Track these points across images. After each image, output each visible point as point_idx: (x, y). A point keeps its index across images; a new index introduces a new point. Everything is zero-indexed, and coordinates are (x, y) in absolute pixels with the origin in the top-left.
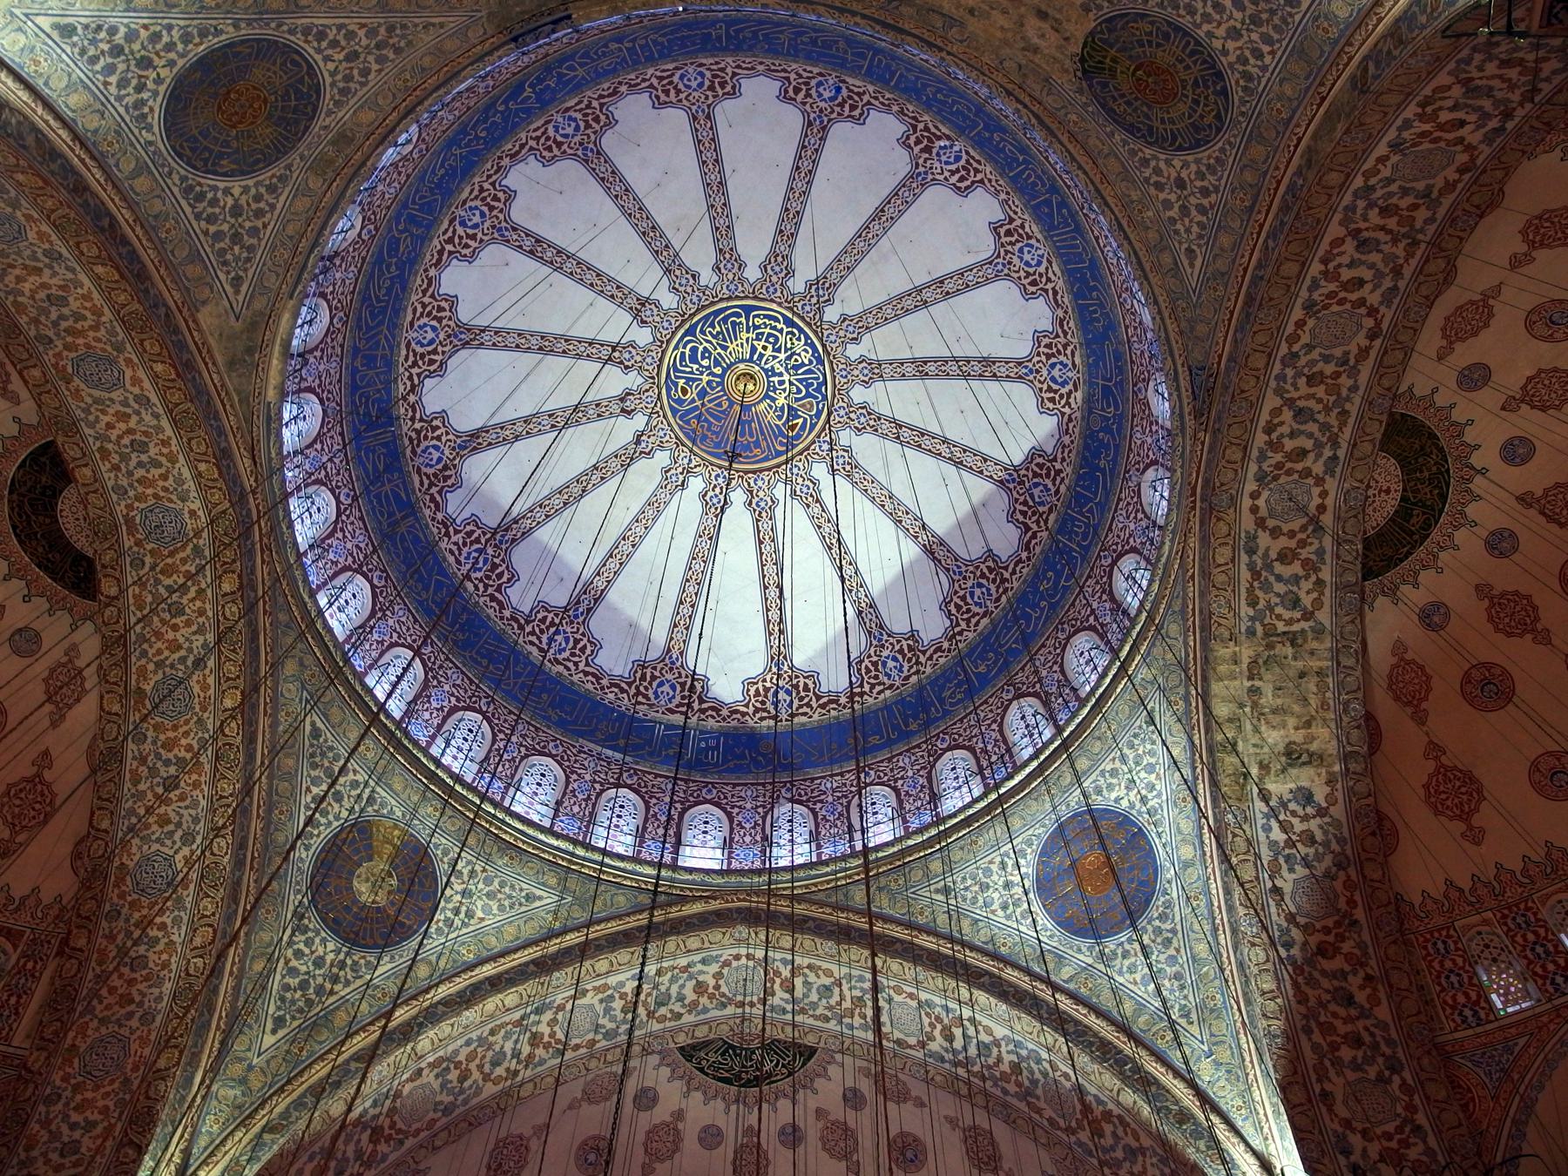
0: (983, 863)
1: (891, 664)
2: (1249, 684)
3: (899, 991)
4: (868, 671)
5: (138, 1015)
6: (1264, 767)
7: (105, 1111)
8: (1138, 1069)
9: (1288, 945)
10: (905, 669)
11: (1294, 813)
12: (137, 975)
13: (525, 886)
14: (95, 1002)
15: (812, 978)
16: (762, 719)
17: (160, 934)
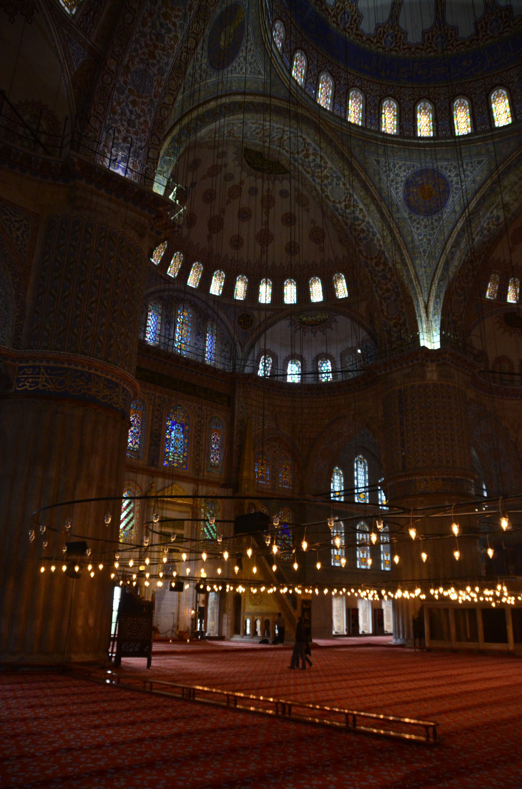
0: (396, 162)
1: (389, 38)
2: (517, 180)
3: (344, 184)
4: (380, 33)
5: (157, 67)
6: (498, 205)
7: (143, 111)
8: (404, 259)
9: (466, 256)
10: (393, 45)
11: (492, 222)
12: (159, 44)
13: (260, 66)
14: (138, 46)
15: (318, 160)
16: (334, 22)
17: (173, 28)
